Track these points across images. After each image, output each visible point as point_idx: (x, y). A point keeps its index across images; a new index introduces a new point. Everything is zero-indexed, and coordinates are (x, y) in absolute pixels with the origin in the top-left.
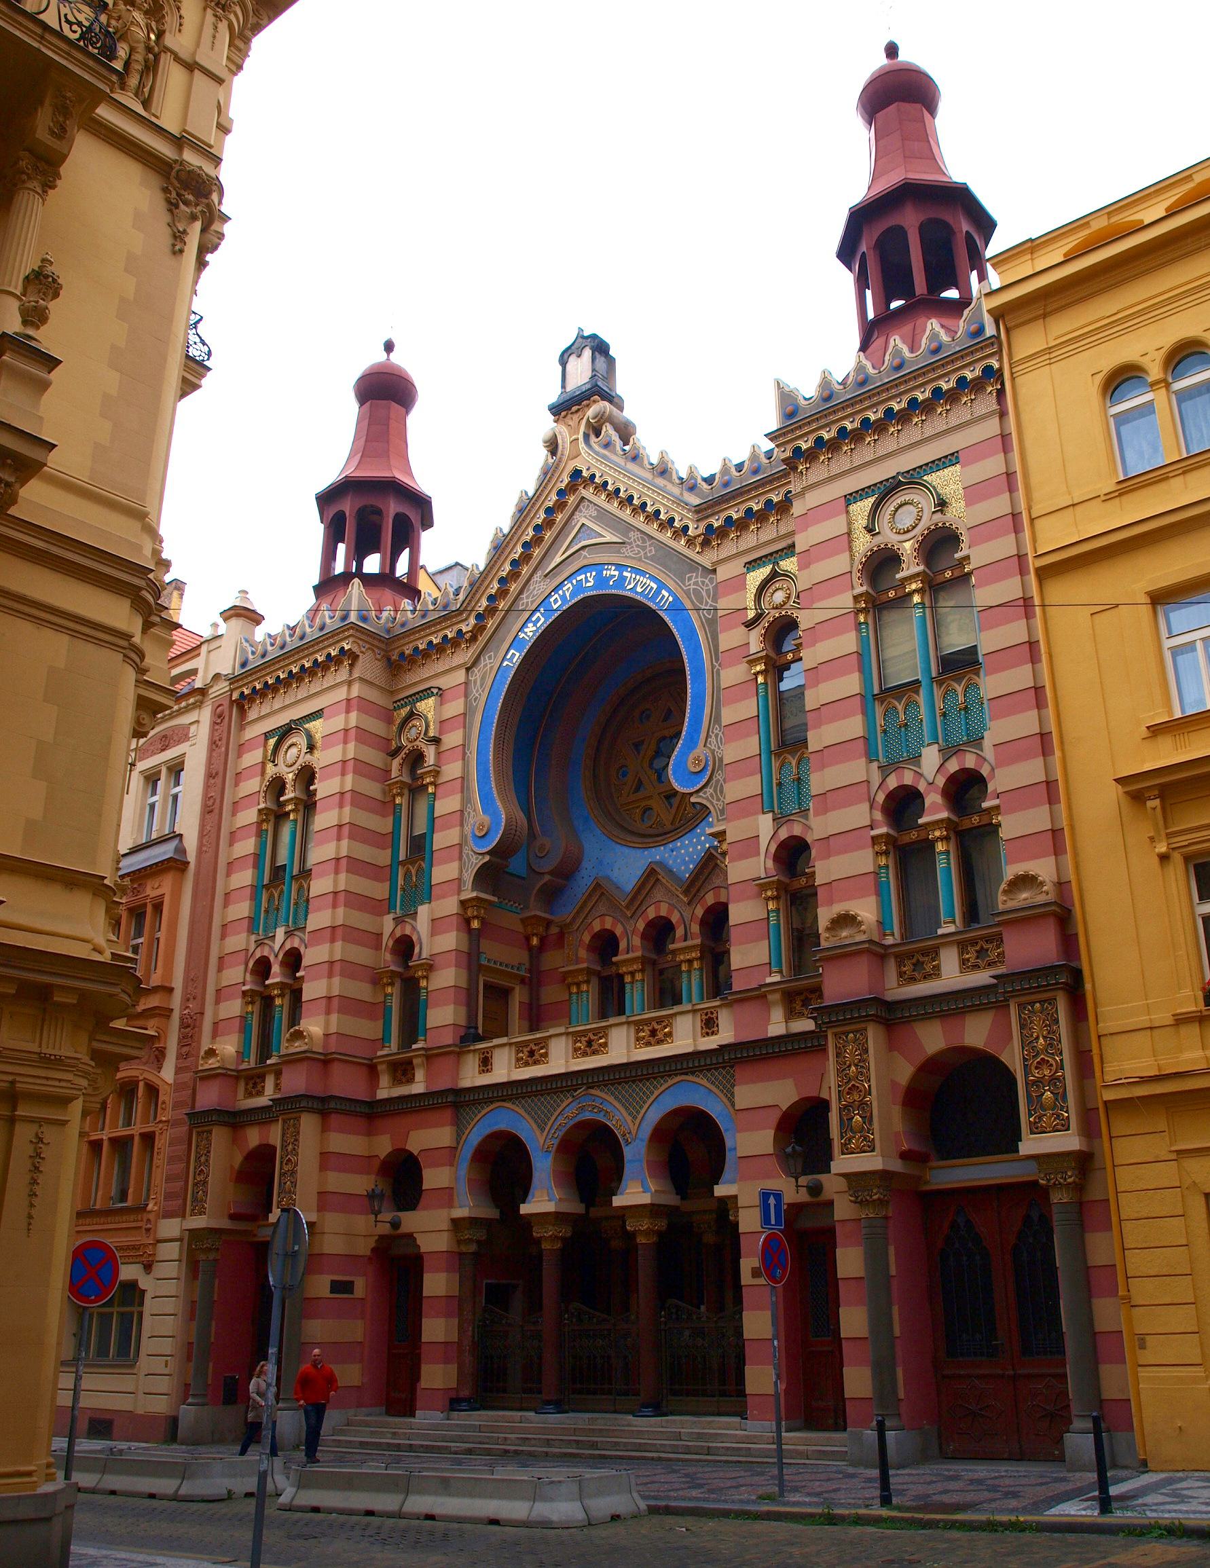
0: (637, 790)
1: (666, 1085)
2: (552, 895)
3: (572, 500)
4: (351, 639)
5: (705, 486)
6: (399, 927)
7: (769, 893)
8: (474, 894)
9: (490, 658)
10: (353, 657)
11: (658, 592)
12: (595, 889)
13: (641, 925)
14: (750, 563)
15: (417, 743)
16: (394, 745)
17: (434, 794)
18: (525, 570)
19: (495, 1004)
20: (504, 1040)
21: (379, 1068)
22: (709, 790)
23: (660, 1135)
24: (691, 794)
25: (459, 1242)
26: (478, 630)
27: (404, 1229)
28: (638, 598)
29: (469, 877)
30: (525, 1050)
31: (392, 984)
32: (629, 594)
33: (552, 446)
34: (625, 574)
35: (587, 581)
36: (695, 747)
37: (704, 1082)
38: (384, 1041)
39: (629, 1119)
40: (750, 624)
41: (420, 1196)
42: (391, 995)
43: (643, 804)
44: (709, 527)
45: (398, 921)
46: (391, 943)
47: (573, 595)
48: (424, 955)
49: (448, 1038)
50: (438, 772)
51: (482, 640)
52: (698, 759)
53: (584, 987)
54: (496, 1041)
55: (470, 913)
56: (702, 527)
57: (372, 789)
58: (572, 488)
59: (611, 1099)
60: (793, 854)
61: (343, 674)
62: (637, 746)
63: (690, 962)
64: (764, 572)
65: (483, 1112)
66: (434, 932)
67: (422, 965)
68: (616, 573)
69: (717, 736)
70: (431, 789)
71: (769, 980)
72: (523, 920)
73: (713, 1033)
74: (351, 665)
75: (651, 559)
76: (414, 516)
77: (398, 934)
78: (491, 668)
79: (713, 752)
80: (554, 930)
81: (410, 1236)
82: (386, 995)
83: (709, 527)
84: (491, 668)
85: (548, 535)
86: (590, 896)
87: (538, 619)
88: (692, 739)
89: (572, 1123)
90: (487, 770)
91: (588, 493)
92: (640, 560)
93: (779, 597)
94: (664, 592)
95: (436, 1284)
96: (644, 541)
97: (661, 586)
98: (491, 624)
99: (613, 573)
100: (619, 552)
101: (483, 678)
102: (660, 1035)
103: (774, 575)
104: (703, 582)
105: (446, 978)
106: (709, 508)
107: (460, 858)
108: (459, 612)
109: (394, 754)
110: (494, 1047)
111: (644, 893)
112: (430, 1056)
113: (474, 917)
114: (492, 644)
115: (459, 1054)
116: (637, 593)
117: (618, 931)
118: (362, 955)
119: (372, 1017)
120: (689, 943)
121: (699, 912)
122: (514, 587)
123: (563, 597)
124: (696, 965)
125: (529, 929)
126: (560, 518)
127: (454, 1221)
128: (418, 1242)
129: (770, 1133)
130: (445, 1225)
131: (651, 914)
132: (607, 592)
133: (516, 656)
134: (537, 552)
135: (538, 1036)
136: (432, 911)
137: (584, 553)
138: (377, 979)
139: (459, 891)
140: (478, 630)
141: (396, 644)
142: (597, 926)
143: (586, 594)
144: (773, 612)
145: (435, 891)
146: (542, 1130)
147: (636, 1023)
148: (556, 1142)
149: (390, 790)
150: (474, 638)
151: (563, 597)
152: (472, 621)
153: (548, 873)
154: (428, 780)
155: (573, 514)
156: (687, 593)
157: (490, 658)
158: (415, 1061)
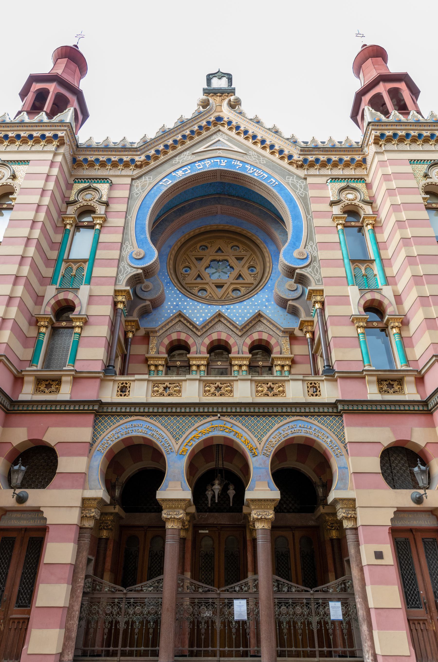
0: (196, 279)
1: (285, 422)
2: (145, 313)
3: (213, 129)
4: (65, 132)
5: (302, 144)
6: (62, 294)
7: (361, 324)
8: (128, 288)
9: (150, 178)
10: (62, 143)
11: (268, 178)
12: (176, 317)
13: (207, 341)
14: (332, 179)
15: (91, 202)
16: (72, 199)
17: (100, 231)
18: (180, 148)
19: (123, 357)
20: (146, 377)
21: (26, 379)
22: (309, 269)
23: (280, 454)
24: (297, 269)
25: (82, 518)
26: (146, 163)
27: (30, 503)
28: (256, 178)
29: (124, 279)
30: (162, 386)
31: (47, 327)
32: (249, 175)
33: (205, 104)
34: (246, 166)
35: (220, 162)
36: (298, 247)
37: (316, 422)
38: (32, 362)
39: (255, 440)
40: (333, 203)
41: (51, 479)
42: (44, 334)
43: (200, 286)
44: (305, 160)
45: (59, 290)
46: (53, 302)
47: (211, 166)
48: (83, 313)
49: (98, 367)
50: (105, 220)
51: (145, 169)
52: (301, 253)
53: (160, 368)
54: (137, 377)
55: (120, 298)
56: (301, 158)
57: (55, 215)
58: (215, 125)
59: (240, 425)
60: (375, 308)
61: (52, 147)
62: (200, 259)
63: (240, 366)
64: (343, 184)
65: (122, 422)
66: (89, 303)
67: (82, 319)
68: (241, 165)
69: (311, 246)
70: (98, 227)
71: (367, 368)
72: (126, 321)
73: (316, 395)
74: (58, 146)
75: (264, 165)
76: (80, 117)
77: (61, 296)
78: (150, 183)
79: (310, 252)
80: (141, 333)
81: (37, 511)
82: (39, 333)
83: (305, 160)
84: (150, 183)
85: (197, 138)
86: (172, 320)
87: (186, 170)
88: (295, 244)
89: (204, 437)
90: (143, 228)
91: (225, 129)
92: (257, 163)
93: (350, 196)
94: (272, 179)
95: (60, 552)
96: (259, 157)
97: (270, 177)
98: (153, 164)
99: (238, 164)
100: (243, 157)
101: (143, 187)
102: (276, 391)
103: (347, 187)
104: (297, 182)
105: (101, 330)
106: (308, 151)
107: (118, 267)
108: (136, 150)
109: (69, 203)
110: (134, 381)
111: (210, 325)
112: (78, 378)
113: (123, 302)
114: (153, 173)
115: (102, 380)
116: (254, 175)
117: (190, 341)
118: (30, 303)
119: (25, 346)
120: (241, 355)
121: (249, 341)
122: (171, 153)
123: (204, 165)
124: (244, 368)
125: (129, 327)
126: (205, 134)
127: (84, 500)
128: (45, 515)
129: (378, 460)
130: (79, 504)
131: (215, 337)
132: (234, 171)
133: (169, 183)
134: (189, 143)
135: (174, 378)
136: (91, 290)
137: (220, 151)
138: (35, 322)
139: (115, 284)
140: (146, 163)
141: (84, 153)
142: (174, 337)
143: (220, 168)
144: (347, 202)
145: (93, 280)
146: (177, 439)
147: (256, 381)
148: (190, 449)
149: (63, 220)
150: (140, 167)
151: (204, 165)
152: (143, 158)
153: (149, 300)
154: (98, 222)
155: (212, 135)
156: (288, 184)
157: (150, 178)
158: (64, 379)
